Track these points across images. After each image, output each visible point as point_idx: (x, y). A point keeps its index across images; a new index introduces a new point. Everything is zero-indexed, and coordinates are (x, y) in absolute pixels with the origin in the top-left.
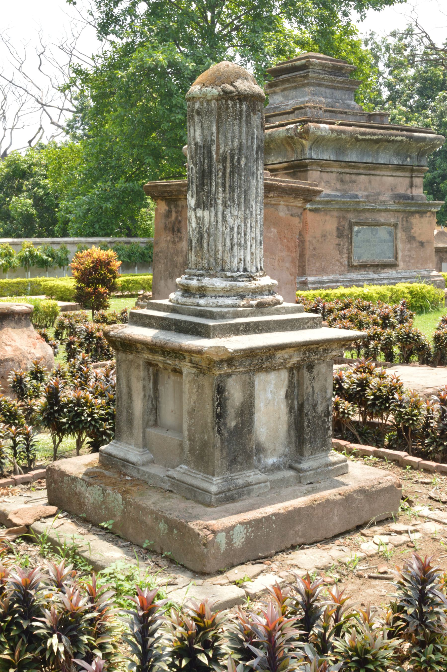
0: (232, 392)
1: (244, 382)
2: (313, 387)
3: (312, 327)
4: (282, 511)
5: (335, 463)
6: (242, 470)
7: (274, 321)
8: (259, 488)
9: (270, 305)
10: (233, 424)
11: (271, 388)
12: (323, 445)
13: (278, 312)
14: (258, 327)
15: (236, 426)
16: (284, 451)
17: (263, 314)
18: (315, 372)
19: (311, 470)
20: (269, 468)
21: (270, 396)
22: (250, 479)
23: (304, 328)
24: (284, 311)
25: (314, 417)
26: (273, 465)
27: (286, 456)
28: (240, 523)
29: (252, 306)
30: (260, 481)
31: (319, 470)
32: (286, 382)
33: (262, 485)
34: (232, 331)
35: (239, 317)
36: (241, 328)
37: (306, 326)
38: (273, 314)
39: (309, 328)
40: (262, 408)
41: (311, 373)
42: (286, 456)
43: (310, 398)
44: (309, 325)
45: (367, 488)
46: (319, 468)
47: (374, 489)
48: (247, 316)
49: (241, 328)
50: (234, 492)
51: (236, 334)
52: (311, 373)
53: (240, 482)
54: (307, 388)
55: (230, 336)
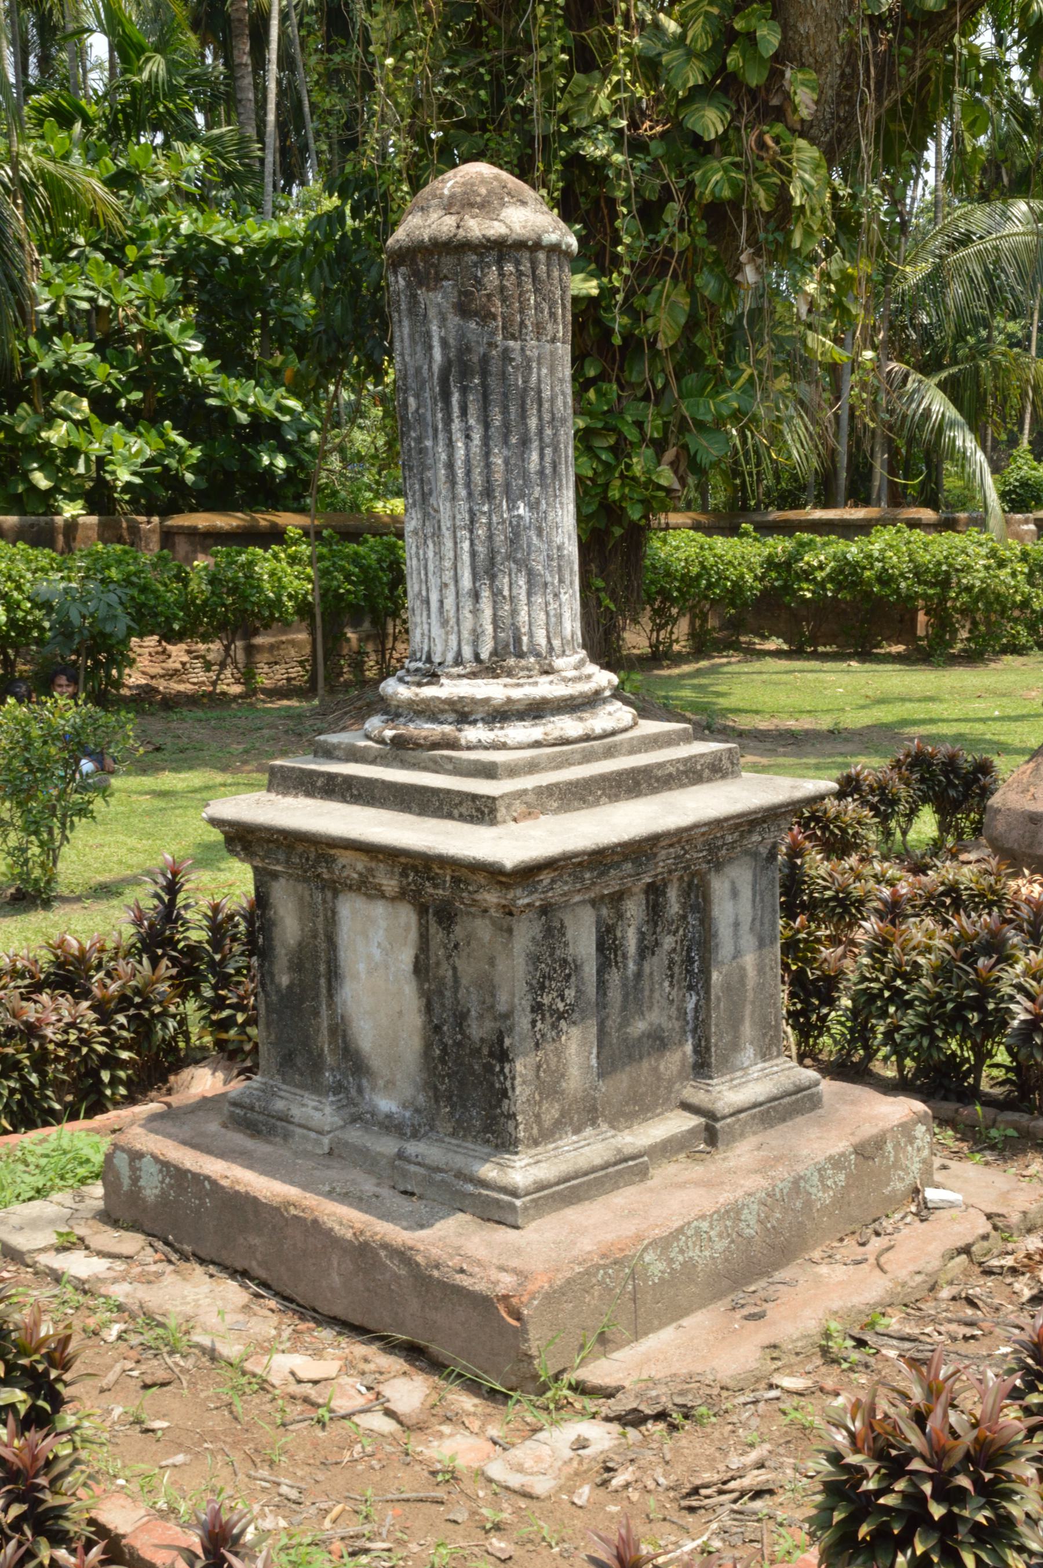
0: (282, 912)
1: (301, 899)
2: (455, 969)
3: (470, 819)
4: (224, 1183)
5: (484, 1184)
6: (303, 1086)
7: (383, 782)
8: (304, 1137)
9: (418, 746)
10: (284, 980)
11: (379, 935)
12: (487, 1129)
13: (436, 767)
14: (350, 788)
15: (290, 987)
16: (414, 1098)
17: (405, 764)
18: (459, 931)
19: (419, 1164)
20: (381, 1118)
21: (377, 953)
22: (296, 1112)
23: (450, 816)
24: (450, 767)
25: (459, 1045)
26: (389, 1116)
27: (417, 1111)
28: (155, 1158)
29: (382, 741)
30: (312, 1124)
31: (438, 1177)
32: (413, 935)
33: (313, 1135)
34: (302, 784)
35: (356, 761)
36: (319, 784)
37: (456, 812)
38: (426, 769)
39: (462, 818)
40: (363, 976)
41: (448, 930)
42: (417, 1111)
43: (448, 994)
44: (463, 810)
45: (419, 1259)
46: (438, 1170)
47: (436, 1273)
48: (373, 762)
49: (319, 784)
50: (261, 1118)
51: (309, 794)
52: (448, 930)
53: (279, 1105)
54: (438, 964)
55: (296, 796)
